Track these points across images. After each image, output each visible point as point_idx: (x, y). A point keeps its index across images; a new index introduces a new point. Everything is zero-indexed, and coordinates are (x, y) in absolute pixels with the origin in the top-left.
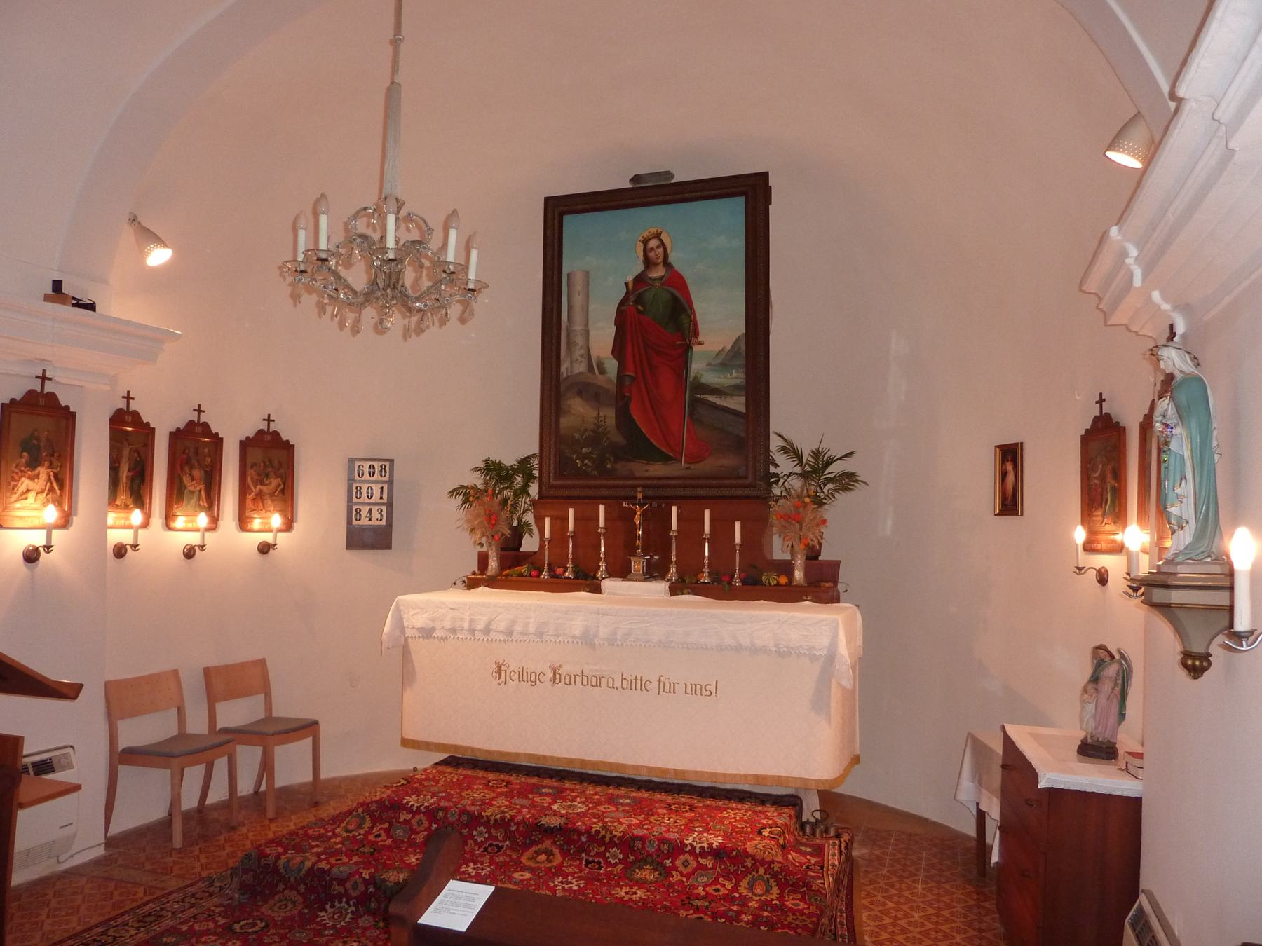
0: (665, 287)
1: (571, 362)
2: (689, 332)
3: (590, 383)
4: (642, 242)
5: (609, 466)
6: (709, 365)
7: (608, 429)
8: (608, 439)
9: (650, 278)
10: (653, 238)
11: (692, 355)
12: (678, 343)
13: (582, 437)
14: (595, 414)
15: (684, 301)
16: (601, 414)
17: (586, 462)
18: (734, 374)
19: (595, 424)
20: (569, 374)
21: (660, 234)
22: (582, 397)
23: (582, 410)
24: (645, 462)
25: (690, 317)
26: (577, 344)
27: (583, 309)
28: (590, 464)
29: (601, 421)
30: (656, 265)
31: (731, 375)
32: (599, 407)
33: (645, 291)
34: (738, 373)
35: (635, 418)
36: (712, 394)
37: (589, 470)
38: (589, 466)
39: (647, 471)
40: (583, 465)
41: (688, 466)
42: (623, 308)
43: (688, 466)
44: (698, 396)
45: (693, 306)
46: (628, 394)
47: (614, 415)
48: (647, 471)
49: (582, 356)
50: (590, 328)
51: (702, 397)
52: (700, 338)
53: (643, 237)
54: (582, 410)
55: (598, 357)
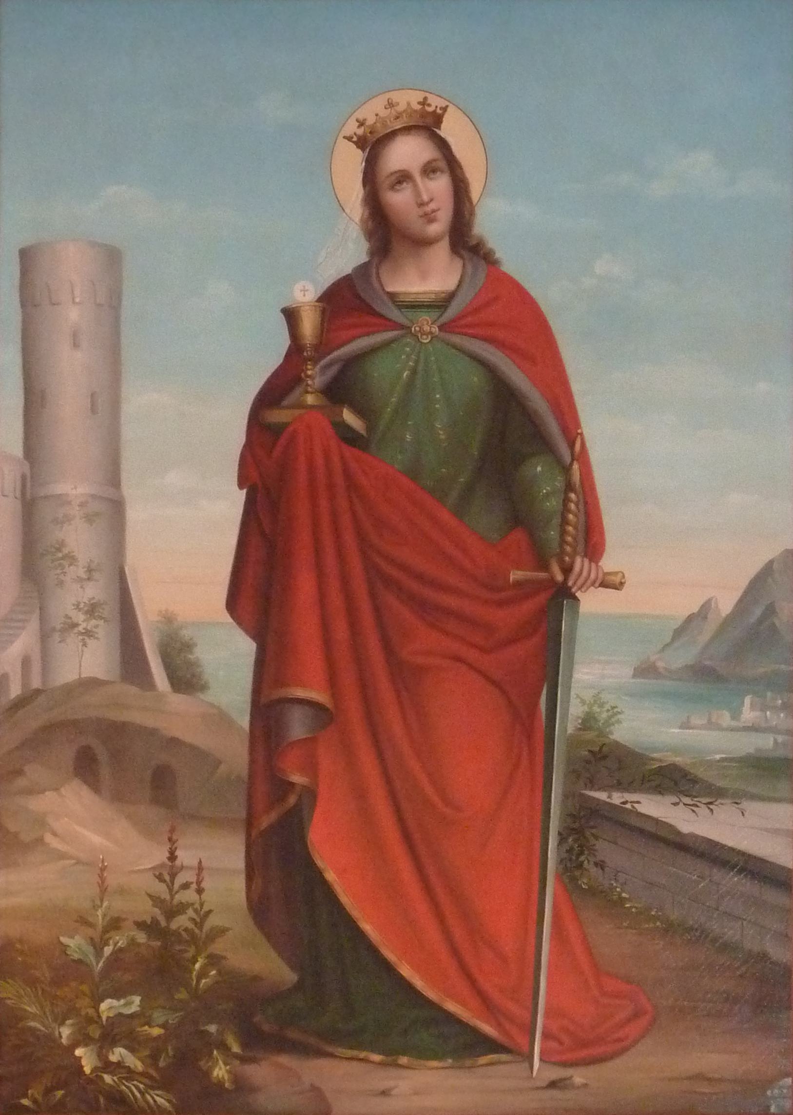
0: (456, 339)
1: (45, 636)
2: (563, 533)
3: (124, 724)
4: (361, 143)
5: (220, 1072)
6: (646, 670)
7: (213, 921)
8: (214, 960)
9: (392, 296)
10: (407, 130)
11: (573, 629)
12: (515, 575)
13: (98, 948)
14: (160, 856)
15: (538, 402)
16: (185, 857)
17: (118, 1054)
18: (748, 715)
19: (156, 900)
20: (36, 683)
21: (438, 119)
22: (95, 786)
23: (96, 839)
24: (377, 1058)
25: (567, 470)
26: (72, 559)
27: (93, 410)
28: (134, 1062)
29: (186, 886)
30: (423, 243)
31: (736, 715)
32: (172, 830)
33: (373, 350)
34: (764, 708)
35: (330, 876)
36: (659, 790)
37: (133, 1089)
38: (129, 1070)
39: (384, 1093)
40: (108, 1066)
41: (556, 1073)
42: (276, 416)
43: (556, 1073)
44: (602, 796)
45: (578, 425)
46: (297, 778)
47: (239, 863)
48: (384, 1093)
49: (92, 610)
50: (129, 490)
51: (617, 798)
52: (609, 563)
53: (361, 124)
54: (96, 839)
55: (168, 619)
